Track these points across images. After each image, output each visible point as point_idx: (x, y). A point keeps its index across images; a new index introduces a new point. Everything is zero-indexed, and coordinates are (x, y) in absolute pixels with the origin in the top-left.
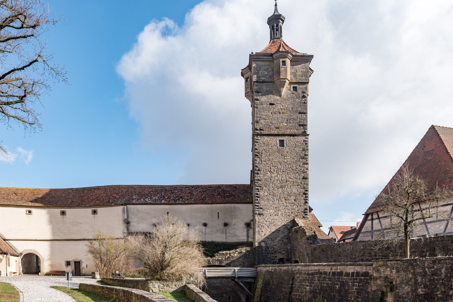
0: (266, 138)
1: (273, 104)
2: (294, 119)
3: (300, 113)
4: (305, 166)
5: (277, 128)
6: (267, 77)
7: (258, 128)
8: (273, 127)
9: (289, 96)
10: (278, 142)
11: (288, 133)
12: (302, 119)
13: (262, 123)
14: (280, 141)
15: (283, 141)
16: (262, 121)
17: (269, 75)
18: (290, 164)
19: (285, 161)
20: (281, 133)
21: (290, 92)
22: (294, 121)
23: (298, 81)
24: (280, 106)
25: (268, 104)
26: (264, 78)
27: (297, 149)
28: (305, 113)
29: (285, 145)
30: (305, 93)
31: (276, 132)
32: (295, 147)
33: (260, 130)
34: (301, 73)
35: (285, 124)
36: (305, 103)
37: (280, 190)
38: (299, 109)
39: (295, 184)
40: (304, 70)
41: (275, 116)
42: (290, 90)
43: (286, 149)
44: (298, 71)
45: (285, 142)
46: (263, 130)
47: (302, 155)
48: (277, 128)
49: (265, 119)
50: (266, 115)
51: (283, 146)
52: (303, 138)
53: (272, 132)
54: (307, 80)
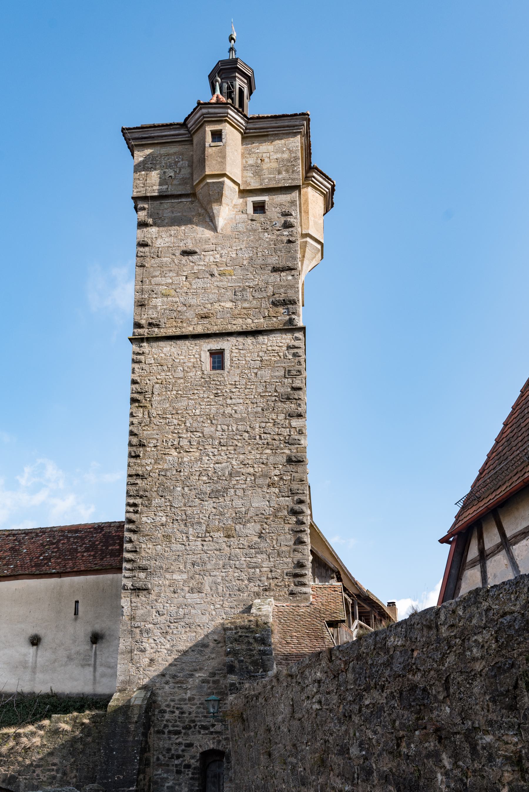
0: (167, 348)
2: (256, 289)
3: (275, 270)
7: (143, 322)
8: (190, 314)
11: (239, 329)
13: (155, 307)
16: (158, 302)
20: (215, 329)
22: (257, 295)
24: (210, 258)
27: (266, 374)
28: (290, 269)
29: (227, 363)
31: (199, 330)
32: (260, 368)
35: (229, 305)
36: (289, 242)
38: (273, 260)
43: (230, 375)
46: (158, 326)
49: (167, 296)
50: (167, 285)
51: (222, 367)
52: (287, 339)
53: (189, 330)
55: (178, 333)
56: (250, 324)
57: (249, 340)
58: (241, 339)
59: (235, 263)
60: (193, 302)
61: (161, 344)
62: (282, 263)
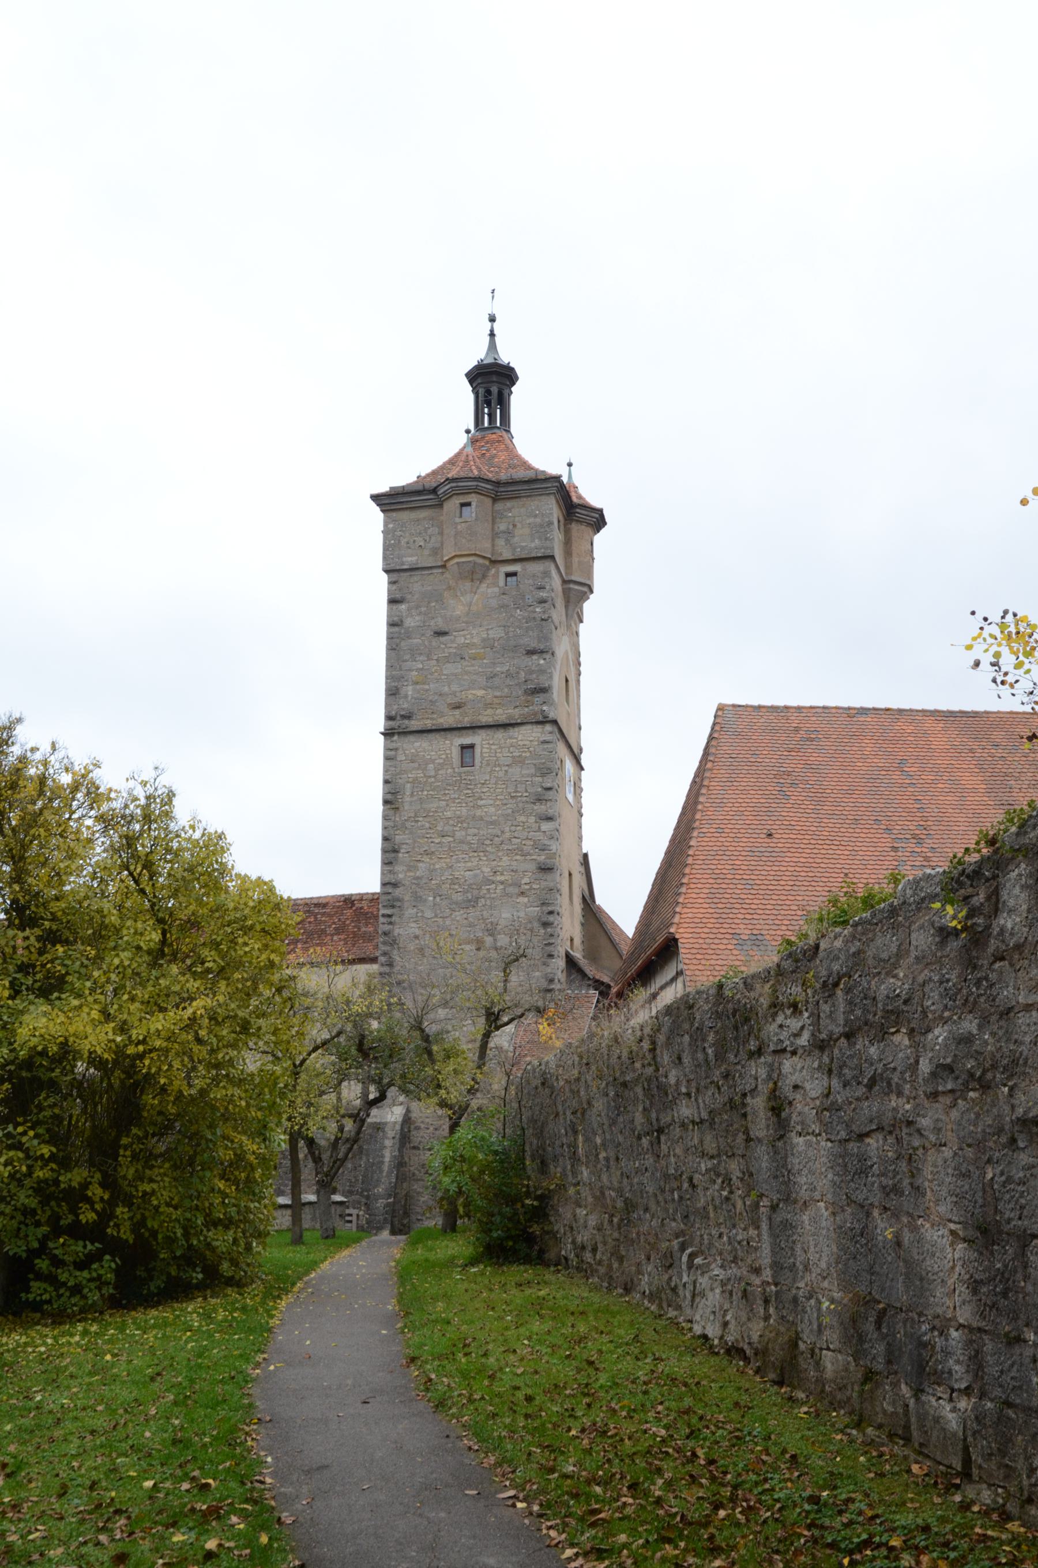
1: (444, 633)
2: (509, 675)
4: (546, 826)
5: (458, 706)
6: (426, 552)
9: (494, 603)
10: (456, 753)
11: (490, 720)
12: (531, 672)
13: (406, 696)
14: (463, 748)
15: (472, 747)
16: (410, 690)
17: (430, 545)
18: (492, 823)
19: (478, 813)
20: (466, 721)
21: (496, 590)
23: (519, 554)
25: (430, 633)
26: (414, 559)
27: (516, 772)
30: (541, 588)
31: (449, 719)
33: (403, 717)
34: (527, 531)
35: (481, 693)
37: (459, 915)
38: (525, 640)
39: (511, 890)
40: (538, 520)
41: (449, 669)
42: (495, 584)
44: (519, 525)
45: (478, 750)
47: (531, 790)
48: (458, 706)
49: (417, 683)
50: (417, 670)
54: (546, 548)
55: (429, 724)
56: (501, 715)
57: (500, 734)
58: (490, 732)
59: (488, 644)
60: (446, 689)
61: (411, 738)
62: (534, 645)
